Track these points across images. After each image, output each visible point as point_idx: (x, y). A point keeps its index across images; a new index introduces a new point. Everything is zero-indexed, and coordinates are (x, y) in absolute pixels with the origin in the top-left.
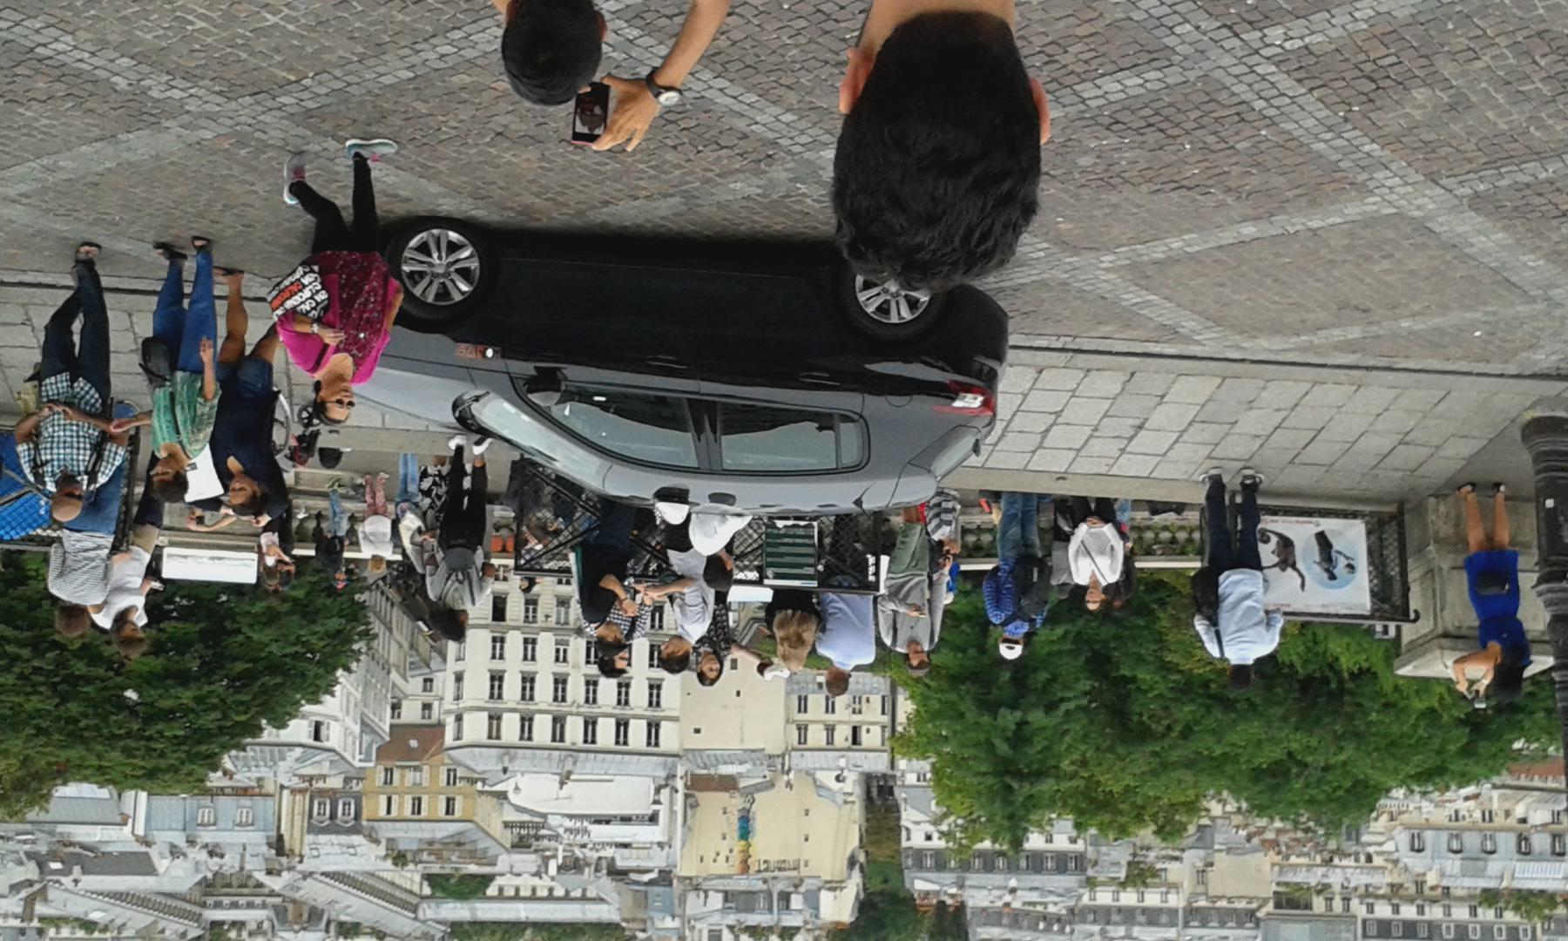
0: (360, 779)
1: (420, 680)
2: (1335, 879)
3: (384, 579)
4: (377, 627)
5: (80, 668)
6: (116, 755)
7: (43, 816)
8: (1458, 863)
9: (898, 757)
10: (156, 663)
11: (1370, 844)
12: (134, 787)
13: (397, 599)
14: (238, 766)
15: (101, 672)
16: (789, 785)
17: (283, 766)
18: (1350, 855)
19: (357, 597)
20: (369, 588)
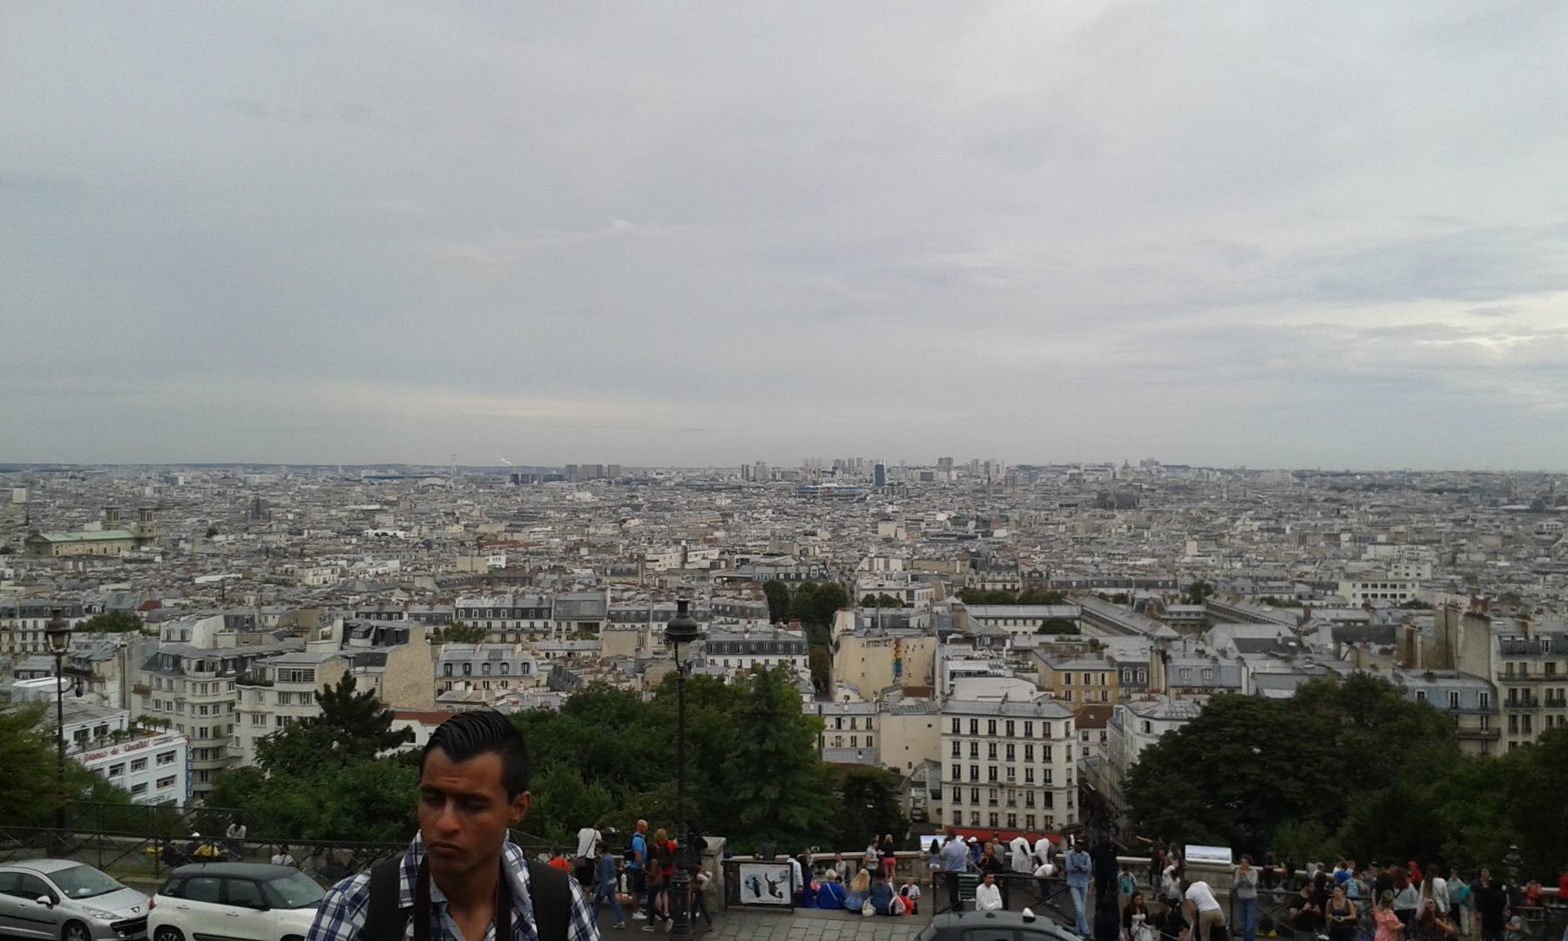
0: (1121, 697)
1: (1091, 755)
2: (567, 644)
3: (1117, 817)
4: (1119, 789)
5: (1287, 766)
6: (1261, 716)
7: (1299, 679)
8: (504, 657)
9: (817, 712)
10: (1243, 769)
11: (548, 664)
12: (1249, 697)
13: (1107, 804)
14: (1189, 708)
15: (1275, 763)
16: (876, 693)
17: (1166, 707)
18: (560, 658)
19: (1132, 808)
20: (1126, 812)
